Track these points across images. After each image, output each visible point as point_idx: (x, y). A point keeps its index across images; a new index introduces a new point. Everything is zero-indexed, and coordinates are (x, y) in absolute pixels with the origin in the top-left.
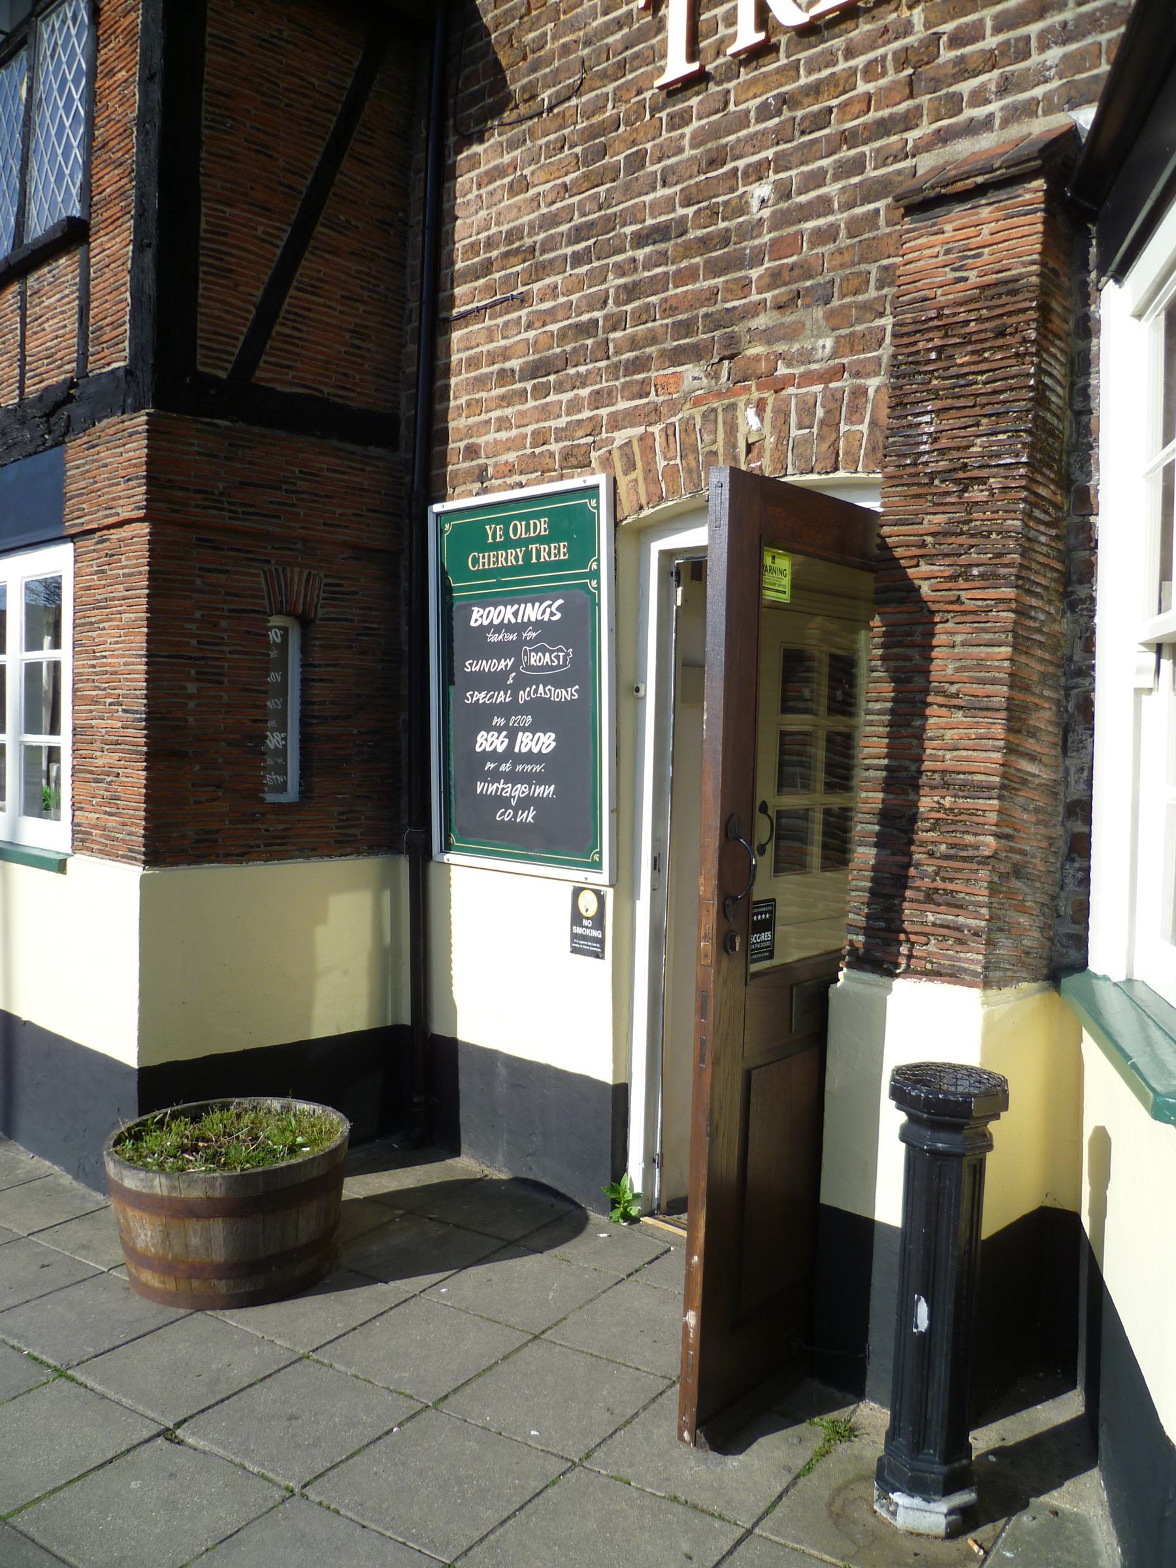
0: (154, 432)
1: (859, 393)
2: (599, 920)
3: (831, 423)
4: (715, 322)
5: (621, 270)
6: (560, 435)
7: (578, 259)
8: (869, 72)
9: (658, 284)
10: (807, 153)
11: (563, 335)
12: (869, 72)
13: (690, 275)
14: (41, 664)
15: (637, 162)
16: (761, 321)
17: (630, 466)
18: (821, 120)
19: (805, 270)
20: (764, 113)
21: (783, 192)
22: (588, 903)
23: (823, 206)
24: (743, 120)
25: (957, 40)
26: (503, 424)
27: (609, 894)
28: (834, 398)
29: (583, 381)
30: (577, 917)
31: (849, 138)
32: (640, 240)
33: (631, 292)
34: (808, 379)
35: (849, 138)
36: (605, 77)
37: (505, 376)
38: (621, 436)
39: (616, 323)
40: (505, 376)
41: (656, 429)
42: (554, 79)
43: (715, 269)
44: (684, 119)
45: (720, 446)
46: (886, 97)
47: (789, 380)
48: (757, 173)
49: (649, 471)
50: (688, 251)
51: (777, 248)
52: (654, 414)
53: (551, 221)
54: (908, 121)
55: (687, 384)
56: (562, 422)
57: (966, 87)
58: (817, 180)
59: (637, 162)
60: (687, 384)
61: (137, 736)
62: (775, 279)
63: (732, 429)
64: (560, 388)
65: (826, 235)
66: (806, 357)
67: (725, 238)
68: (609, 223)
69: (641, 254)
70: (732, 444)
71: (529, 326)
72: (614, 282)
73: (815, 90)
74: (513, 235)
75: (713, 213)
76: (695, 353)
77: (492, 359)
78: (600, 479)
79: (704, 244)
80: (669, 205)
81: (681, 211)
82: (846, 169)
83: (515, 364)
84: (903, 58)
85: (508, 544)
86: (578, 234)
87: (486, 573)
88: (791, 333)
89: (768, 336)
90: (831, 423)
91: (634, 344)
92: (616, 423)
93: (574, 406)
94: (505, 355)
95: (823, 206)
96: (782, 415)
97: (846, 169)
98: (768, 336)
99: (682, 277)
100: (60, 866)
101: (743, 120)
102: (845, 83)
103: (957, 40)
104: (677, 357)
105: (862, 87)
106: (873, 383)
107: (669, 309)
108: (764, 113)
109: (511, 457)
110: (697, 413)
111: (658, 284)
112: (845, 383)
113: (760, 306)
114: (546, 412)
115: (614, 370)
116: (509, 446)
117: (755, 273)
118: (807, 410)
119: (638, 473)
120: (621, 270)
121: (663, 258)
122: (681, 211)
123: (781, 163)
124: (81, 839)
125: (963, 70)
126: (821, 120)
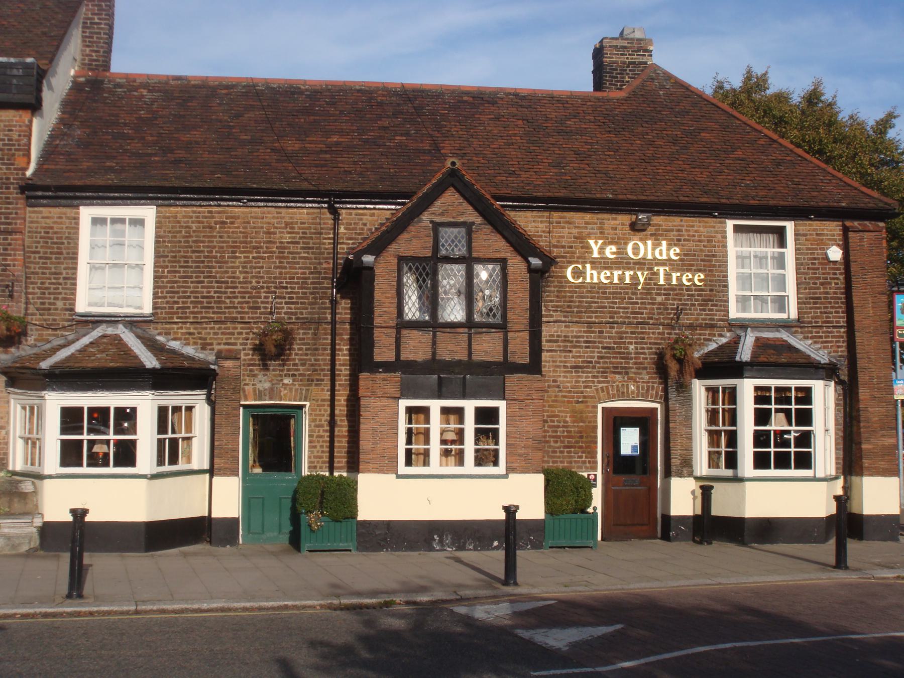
1: (653, 387)
3: (648, 390)
4: (622, 368)
5: (598, 352)
7: (586, 347)
8: (653, 333)
9: (609, 358)
10: (641, 343)
11: (583, 362)
12: (653, 333)
13: (616, 358)
14: (82, 408)
16: (633, 370)
17: (603, 391)
18: (644, 338)
19: (641, 363)
21: (636, 348)
23: (644, 353)
24: (627, 333)
26: (565, 377)
28: (648, 387)
29: (590, 372)
31: (650, 343)
32: (604, 348)
34: (643, 382)
36: (592, 312)
37: (565, 367)
38: (600, 385)
39: (599, 363)
40: (565, 367)
42: (578, 307)
43: (622, 358)
44: (613, 328)
45: (625, 390)
46: (655, 339)
47: (639, 382)
48: (631, 343)
50: (616, 353)
51: (636, 358)
52: (608, 382)
53: (579, 337)
55: (617, 378)
56: (584, 379)
58: (643, 348)
60: (617, 378)
62: (636, 363)
63: (628, 388)
64: (583, 372)
65: (644, 358)
66: (642, 378)
67: (624, 353)
68: (595, 342)
69: (604, 351)
71: (573, 357)
72: (596, 355)
73: (643, 333)
74: (565, 336)
75: (621, 348)
76: (619, 373)
77: (561, 362)
79: (620, 353)
80: (610, 343)
82: (648, 348)
83: (569, 365)
84: (659, 333)
86: (586, 342)
88: (640, 374)
89: (635, 373)
90: (648, 390)
91: (603, 368)
92: (599, 382)
93: (587, 377)
94: (565, 362)
95: (644, 353)
96: (638, 387)
97: (648, 348)
98: (635, 373)
99: (614, 358)
100: (505, 476)
101: (627, 333)
105: (651, 335)
106: (655, 385)
107: (611, 363)
108: (632, 333)
110: (620, 384)
111: (609, 358)
112: (650, 384)
113: (632, 368)
114: (579, 377)
115: (598, 372)
116: (568, 382)
119: (605, 393)
120: (598, 352)
121: (609, 353)
123: (636, 343)
124: (510, 469)
126: (644, 338)
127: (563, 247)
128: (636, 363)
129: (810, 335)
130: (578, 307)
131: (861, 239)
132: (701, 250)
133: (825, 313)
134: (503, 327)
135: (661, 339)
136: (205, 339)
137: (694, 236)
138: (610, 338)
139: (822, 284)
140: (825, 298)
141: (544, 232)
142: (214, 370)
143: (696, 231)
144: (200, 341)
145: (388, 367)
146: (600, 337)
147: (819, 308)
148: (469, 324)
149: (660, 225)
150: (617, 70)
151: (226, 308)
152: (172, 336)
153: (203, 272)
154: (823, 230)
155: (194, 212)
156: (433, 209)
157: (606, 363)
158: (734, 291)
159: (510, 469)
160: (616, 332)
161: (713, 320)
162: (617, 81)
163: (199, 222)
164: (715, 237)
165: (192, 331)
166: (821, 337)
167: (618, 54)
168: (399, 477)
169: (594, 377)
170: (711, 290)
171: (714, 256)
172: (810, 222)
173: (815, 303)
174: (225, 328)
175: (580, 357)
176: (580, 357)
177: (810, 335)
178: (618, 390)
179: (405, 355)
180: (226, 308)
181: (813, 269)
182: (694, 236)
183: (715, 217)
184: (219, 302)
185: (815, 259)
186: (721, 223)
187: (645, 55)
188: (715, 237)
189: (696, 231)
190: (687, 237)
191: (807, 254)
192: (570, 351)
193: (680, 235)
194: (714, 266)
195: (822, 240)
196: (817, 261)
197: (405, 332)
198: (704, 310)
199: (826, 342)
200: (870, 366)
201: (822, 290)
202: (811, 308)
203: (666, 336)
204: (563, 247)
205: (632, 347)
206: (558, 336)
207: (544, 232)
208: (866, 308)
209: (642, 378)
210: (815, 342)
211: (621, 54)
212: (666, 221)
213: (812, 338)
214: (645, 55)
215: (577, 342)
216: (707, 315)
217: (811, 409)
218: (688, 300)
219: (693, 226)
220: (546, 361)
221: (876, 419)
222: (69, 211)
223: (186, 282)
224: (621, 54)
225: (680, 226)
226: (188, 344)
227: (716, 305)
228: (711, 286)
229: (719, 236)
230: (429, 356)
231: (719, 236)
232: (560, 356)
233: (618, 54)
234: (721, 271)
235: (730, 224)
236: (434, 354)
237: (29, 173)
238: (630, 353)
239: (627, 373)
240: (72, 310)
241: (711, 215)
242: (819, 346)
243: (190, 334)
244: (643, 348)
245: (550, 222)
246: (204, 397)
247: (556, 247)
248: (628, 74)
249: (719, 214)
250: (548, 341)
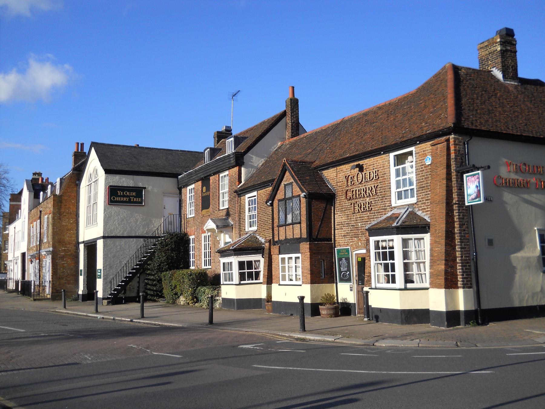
0: (310, 244)
2: (352, 288)
5: (350, 228)
6: (346, 242)
7: (347, 226)
9: (353, 230)
10: (362, 222)
11: (346, 233)
15: (351, 219)
16: (360, 235)
18: (363, 219)
20: (360, 217)
22: (351, 286)
25: (371, 216)
26: (342, 240)
27: (353, 285)
29: (348, 238)
30: (350, 288)
31: (365, 222)
33: (351, 230)
34: (363, 241)
35: (365, 222)
37: (341, 236)
38: (351, 243)
39: (350, 233)
40: (341, 236)
41: (354, 243)
42: (344, 208)
43: (357, 230)
48: (359, 222)
49: (353, 247)
53: (344, 222)
54: (368, 221)
56: (346, 241)
57: (371, 220)
58: (363, 224)
59: (351, 219)
61: (309, 272)
62: (361, 232)
66: (363, 239)
67: (357, 228)
69: (352, 227)
70: (359, 245)
73: (362, 217)
74: (341, 222)
75: (356, 225)
78: (349, 247)
79: (356, 228)
81: (354, 224)
85: (342, 252)
86: (347, 224)
87: (341, 255)
89: (361, 237)
92: (351, 242)
93: (347, 240)
94: (341, 234)
96: (362, 243)
99: (355, 230)
100: (301, 285)
102: (364, 217)
103: (371, 216)
104: (355, 237)
105: (365, 218)
108: (360, 217)
109: (343, 244)
111: (353, 230)
117: (359, 231)
118: (363, 243)
120: (350, 228)
122: (354, 224)
123: (361, 222)
124: (303, 283)
125: (371, 219)
126: (363, 219)
127: (340, 182)
128: (361, 232)
129: (421, 208)
130: (344, 208)
131: (437, 149)
132: (381, 172)
133: (427, 195)
134: (300, 223)
135: (368, 219)
136: (265, 236)
137: (378, 166)
138: (353, 221)
139: (425, 178)
140: (427, 186)
141: (335, 177)
142: (264, 247)
143: (379, 163)
144: (265, 237)
145: (277, 242)
146: (351, 221)
147: (424, 192)
148: (293, 224)
149: (367, 164)
150: (484, 60)
151: (269, 224)
152: (260, 236)
153: (264, 212)
154: (426, 148)
155: (263, 191)
156: (284, 179)
157: (352, 233)
158: (394, 190)
159: (303, 283)
160: (355, 218)
161: (385, 206)
162: (486, 66)
163: (264, 195)
164: (385, 164)
165: (263, 233)
166: (425, 209)
167: (484, 51)
168: (279, 285)
169: (349, 240)
170: (384, 192)
171: (385, 174)
172: (418, 146)
173: (422, 190)
174: (269, 231)
175: (345, 231)
176: (345, 231)
177: (421, 208)
178: (356, 245)
179: (281, 238)
180: (269, 224)
181: (422, 171)
182: (378, 166)
183: (383, 154)
184: (267, 222)
185: (422, 165)
186: (387, 156)
187: (496, 46)
188: (385, 164)
189: (379, 163)
190: (376, 167)
191: (419, 163)
192: (343, 229)
193: (374, 167)
194: (385, 179)
195: (425, 154)
196: (423, 166)
197: (280, 228)
198: (382, 202)
199: (427, 211)
200: (436, 223)
201: (425, 182)
202: (421, 193)
203: (370, 217)
204: (340, 182)
205: (360, 224)
206: (340, 223)
207: (335, 177)
208: (436, 189)
209: (363, 239)
210: (423, 212)
211: (486, 50)
212: (369, 161)
213: (422, 210)
214: (496, 46)
215: (345, 224)
216: (383, 204)
217: (394, 251)
218: (377, 198)
219: (378, 161)
220: (337, 234)
221: (436, 254)
222: (244, 197)
223: (262, 216)
224: (486, 50)
225: (374, 162)
226: (263, 238)
227: (386, 199)
228: (384, 189)
229: (387, 163)
230: (284, 238)
231: (387, 163)
232: (340, 231)
233: (484, 51)
234: (388, 181)
235: (392, 155)
236: (286, 236)
237: (238, 187)
238: (359, 227)
239: (358, 237)
240: (245, 230)
241: (380, 154)
242: (425, 213)
243: (263, 234)
244: (363, 224)
245: (337, 172)
246: (261, 257)
247: (339, 182)
248: (490, 60)
249: (384, 152)
250: (337, 225)
